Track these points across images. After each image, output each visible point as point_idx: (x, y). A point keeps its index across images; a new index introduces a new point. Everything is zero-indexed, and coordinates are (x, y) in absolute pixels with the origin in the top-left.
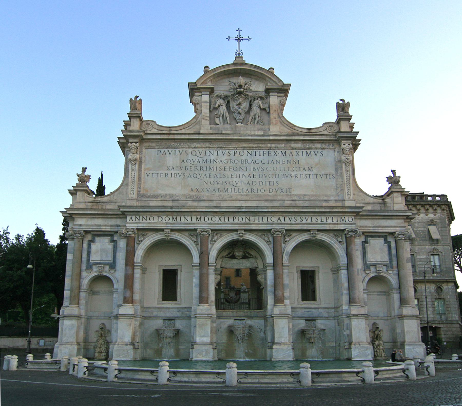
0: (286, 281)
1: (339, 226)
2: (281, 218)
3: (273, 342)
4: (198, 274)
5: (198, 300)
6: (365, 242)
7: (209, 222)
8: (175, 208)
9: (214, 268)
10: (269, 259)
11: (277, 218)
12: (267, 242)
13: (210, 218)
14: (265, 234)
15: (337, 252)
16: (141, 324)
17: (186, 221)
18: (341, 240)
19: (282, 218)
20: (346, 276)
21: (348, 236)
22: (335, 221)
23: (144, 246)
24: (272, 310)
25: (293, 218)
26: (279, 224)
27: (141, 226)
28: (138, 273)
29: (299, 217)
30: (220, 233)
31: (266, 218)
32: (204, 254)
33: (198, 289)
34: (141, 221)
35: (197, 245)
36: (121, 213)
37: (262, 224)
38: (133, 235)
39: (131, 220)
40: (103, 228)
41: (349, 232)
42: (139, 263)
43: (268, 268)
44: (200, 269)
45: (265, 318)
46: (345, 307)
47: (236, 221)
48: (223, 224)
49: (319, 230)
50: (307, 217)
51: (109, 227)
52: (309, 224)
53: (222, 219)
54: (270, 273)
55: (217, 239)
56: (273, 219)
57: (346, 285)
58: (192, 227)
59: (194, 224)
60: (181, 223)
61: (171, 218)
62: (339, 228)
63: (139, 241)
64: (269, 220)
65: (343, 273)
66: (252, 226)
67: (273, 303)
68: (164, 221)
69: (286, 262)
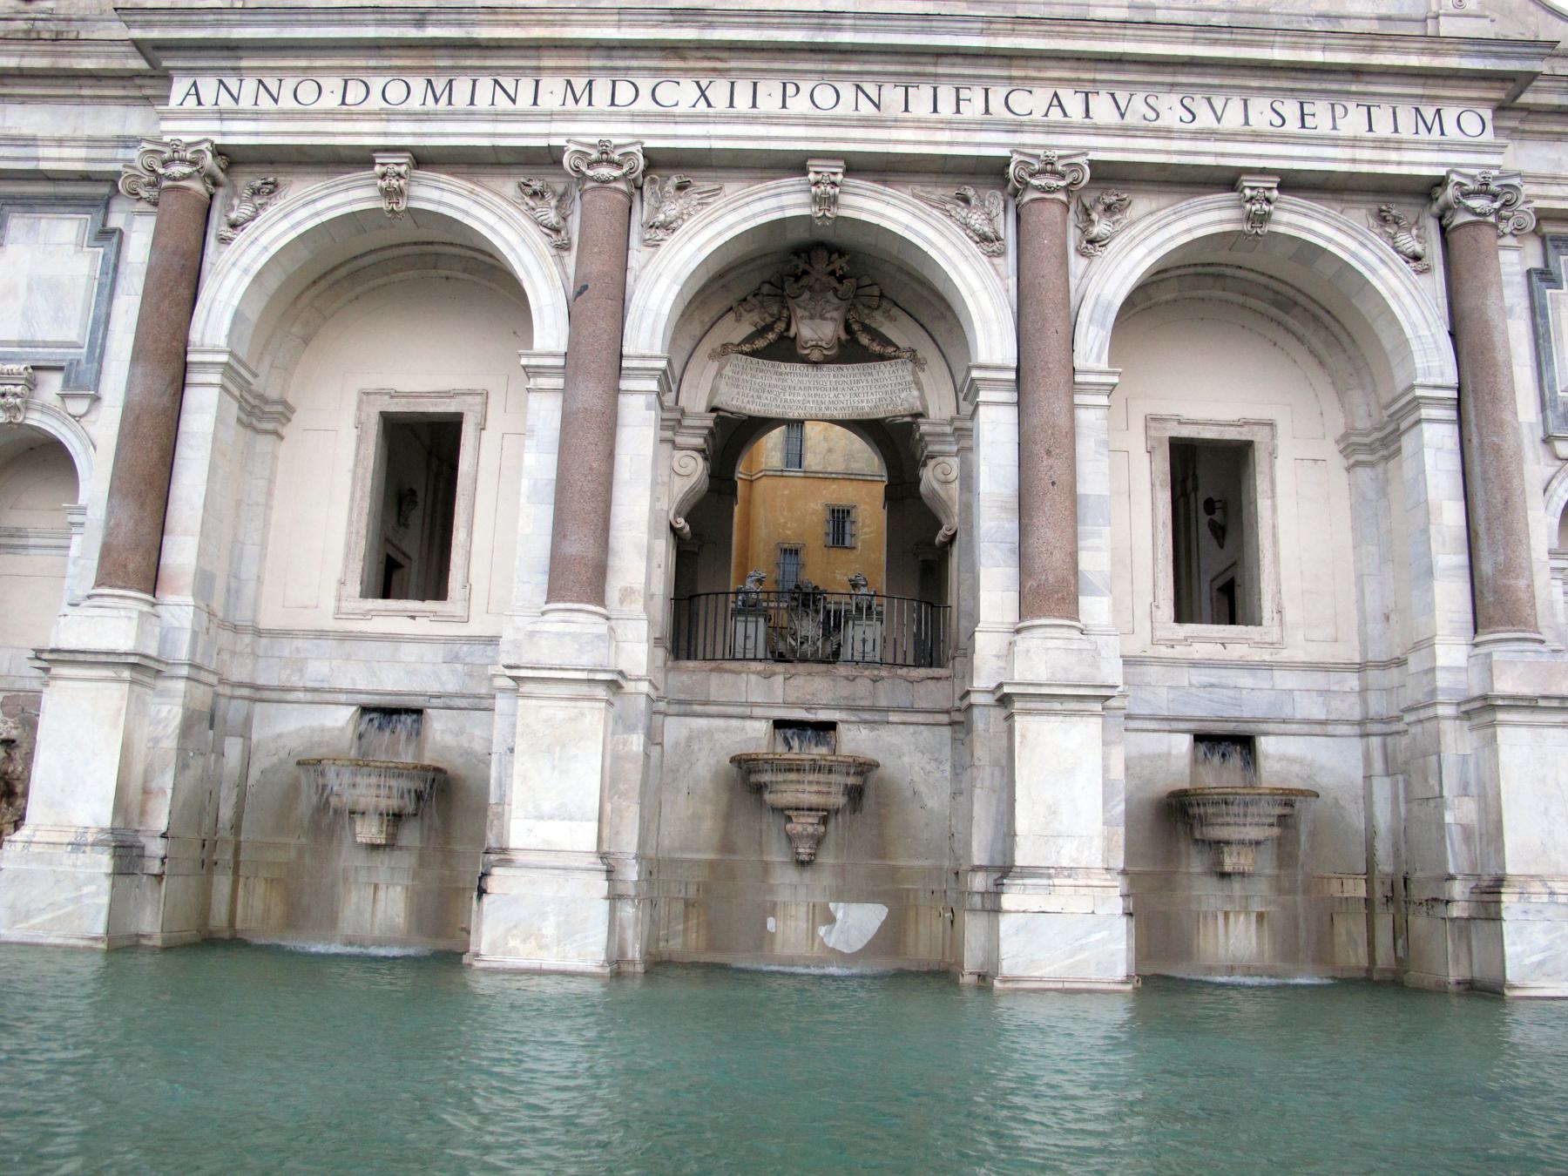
1: (1407, 156)
3: (1004, 871)
4: (556, 423)
5: (542, 580)
6: (1544, 276)
7: (635, 107)
8: (439, 24)
9: (653, 385)
11: (1042, 96)
12: (984, 239)
13: (645, 85)
14: (970, 192)
15: (1394, 320)
16: (204, 725)
17: (503, 103)
18: (1418, 248)
19: (1073, 102)
20: (1453, 463)
21: (1461, 218)
22: (1383, 129)
24: (1009, 653)
26: (1051, 128)
27: (241, 134)
28: (203, 408)
29: (1174, 99)
31: (977, 95)
32: (601, 299)
33: (546, 513)
34: (246, 103)
35: (563, 247)
36: (138, 64)
37: (948, 125)
39: (192, 101)
40: (52, 159)
41: (1466, 195)
43: (983, 396)
44: (566, 393)
46: (1451, 652)
49: (1292, 183)
50: (1218, 102)
51: (82, 153)
52: (1231, 137)
54: (996, 428)
56: (1021, 101)
57: (1450, 515)
59: (551, 116)
60: (470, 115)
61: (418, 84)
62: (1405, 170)
63: (234, 226)
65: (1436, 442)
67: (1011, 615)
68: (375, 102)
69: (1092, 364)
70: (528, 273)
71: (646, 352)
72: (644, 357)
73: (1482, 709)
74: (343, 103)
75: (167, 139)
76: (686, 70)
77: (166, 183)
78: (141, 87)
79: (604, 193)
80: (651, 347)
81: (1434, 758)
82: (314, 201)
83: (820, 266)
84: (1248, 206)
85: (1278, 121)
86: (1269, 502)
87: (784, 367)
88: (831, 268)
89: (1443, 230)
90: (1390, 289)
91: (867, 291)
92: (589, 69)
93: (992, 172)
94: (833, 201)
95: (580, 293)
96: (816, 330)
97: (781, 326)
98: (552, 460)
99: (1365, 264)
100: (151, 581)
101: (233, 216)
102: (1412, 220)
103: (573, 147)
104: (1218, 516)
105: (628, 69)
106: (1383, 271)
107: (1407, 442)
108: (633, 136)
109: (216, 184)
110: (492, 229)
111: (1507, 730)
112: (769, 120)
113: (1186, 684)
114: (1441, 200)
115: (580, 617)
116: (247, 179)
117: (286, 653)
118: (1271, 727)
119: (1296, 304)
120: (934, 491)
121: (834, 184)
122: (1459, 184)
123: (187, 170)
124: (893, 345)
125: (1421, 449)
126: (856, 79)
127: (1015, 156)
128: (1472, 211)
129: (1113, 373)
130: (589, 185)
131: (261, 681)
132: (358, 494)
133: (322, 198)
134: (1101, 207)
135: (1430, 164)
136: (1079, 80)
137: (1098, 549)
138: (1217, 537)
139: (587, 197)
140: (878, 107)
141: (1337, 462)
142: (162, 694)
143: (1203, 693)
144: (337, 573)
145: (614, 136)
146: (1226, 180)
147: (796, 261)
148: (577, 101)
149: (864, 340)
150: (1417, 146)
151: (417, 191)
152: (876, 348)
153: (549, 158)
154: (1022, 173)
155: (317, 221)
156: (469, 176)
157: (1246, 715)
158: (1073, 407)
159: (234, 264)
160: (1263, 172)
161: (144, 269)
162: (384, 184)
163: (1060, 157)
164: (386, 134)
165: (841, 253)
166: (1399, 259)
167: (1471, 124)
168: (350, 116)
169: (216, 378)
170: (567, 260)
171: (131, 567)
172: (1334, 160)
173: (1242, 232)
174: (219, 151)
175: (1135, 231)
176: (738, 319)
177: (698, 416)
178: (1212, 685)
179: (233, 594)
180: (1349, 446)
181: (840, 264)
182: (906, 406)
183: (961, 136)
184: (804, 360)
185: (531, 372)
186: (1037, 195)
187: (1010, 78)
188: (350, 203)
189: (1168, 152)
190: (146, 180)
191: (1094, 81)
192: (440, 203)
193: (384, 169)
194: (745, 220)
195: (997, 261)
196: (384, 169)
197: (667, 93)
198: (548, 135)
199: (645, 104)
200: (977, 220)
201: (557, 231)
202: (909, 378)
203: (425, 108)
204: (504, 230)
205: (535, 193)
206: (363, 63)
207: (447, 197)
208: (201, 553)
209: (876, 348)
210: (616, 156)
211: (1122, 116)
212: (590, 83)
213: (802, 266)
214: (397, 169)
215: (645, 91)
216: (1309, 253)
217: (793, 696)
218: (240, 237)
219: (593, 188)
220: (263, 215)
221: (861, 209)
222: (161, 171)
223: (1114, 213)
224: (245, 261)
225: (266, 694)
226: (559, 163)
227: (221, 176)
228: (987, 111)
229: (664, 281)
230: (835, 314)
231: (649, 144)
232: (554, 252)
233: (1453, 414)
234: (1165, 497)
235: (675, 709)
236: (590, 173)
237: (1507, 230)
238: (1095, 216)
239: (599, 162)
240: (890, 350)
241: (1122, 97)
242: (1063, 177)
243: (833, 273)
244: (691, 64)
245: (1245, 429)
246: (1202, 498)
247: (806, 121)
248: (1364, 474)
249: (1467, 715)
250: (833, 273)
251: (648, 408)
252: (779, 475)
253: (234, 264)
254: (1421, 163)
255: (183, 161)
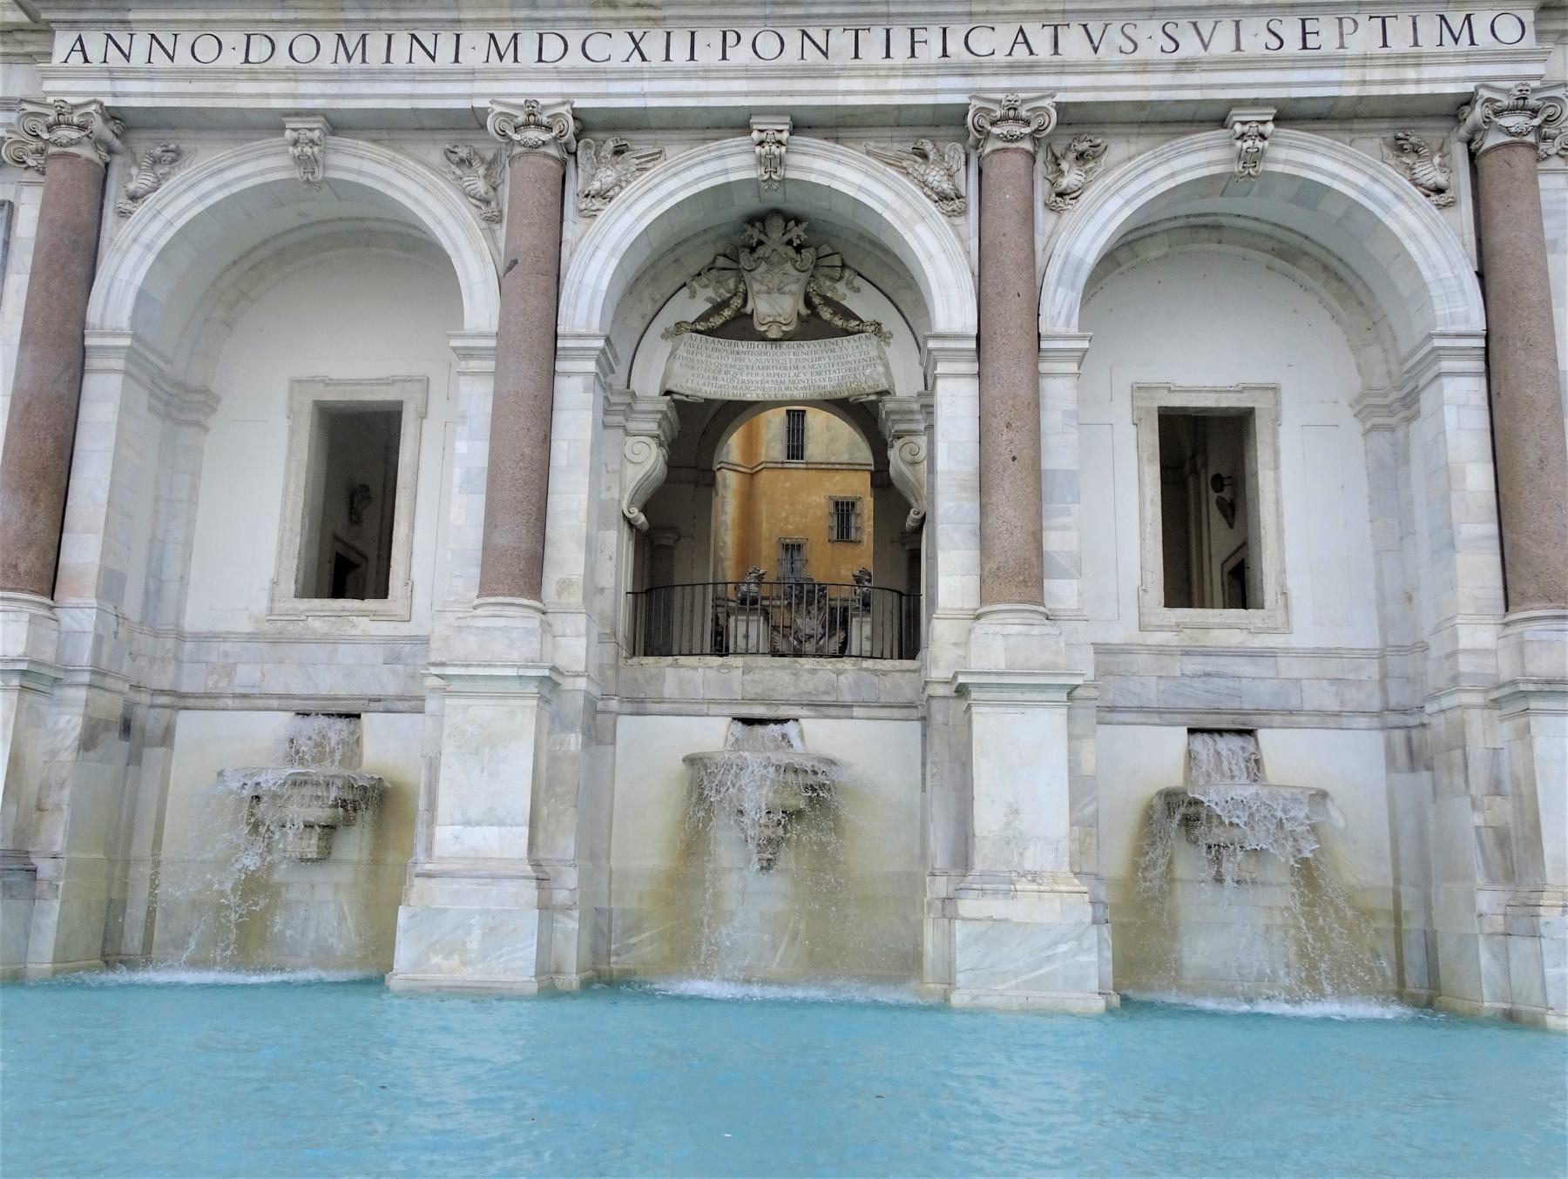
0: (1059, 453)
1: (1427, 72)
2: (1033, 30)
5: (475, 572)
9: (591, 366)
10: (952, 306)
11: (1006, 33)
12: (943, 197)
15: (1411, 264)
18: (1441, 180)
21: (1491, 140)
23: (156, 226)
25: (1115, 28)
26: (1013, 68)
27: (136, 94)
29: (1156, 26)
30: (641, 144)
31: (934, 37)
33: (479, 502)
34: (138, 59)
35: (493, 219)
37: (906, 72)
38: (86, 152)
39: (77, 58)
42: (117, 333)
43: (941, 368)
44: (497, 374)
45: (917, 709)
47: (741, 55)
48: (657, 75)
49: (1288, 115)
52: (1222, 64)
53: (653, 45)
54: (956, 402)
55: (618, 184)
56: (981, 42)
57: (1478, 479)
58: (452, 95)
61: (328, 40)
62: (1425, 89)
63: (134, 198)
64: (955, 45)
66: (842, 84)
67: (972, 602)
69: (1060, 329)
70: (457, 249)
71: (583, 331)
72: (580, 336)
73: (1515, 698)
74: (247, 61)
75: (50, 100)
76: (618, 20)
77: (52, 150)
78: (22, 43)
79: (531, 158)
80: (588, 324)
81: (1458, 752)
82: (221, 171)
83: (776, 233)
84: (1239, 143)
85: (1275, 43)
86: (1271, 474)
87: (743, 346)
88: (786, 238)
89: (1472, 156)
90: (1406, 227)
91: (826, 262)
92: (514, 20)
93: (950, 120)
94: (781, 161)
95: (509, 269)
96: (774, 304)
97: (737, 302)
98: (483, 447)
99: (1377, 201)
100: (49, 582)
101: (132, 186)
102: (1436, 147)
103: (498, 109)
104: (1227, 494)
105: (556, 20)
106: (1399, 208)
107: (1427, 400)
108: (563, 95)
109: (110, 152)
110: (416, 200)
111: (1544, 720)
112: (706, 74)
113: (1178, 674)
114: (1469, 122)
115: (510, 611)
116: (145, 145)
117: (213, 658)
118: (1277, 719)
119: (1306, 253)
120: (901, 475)
121: (780, 143)
122: (1488, 100)
123: (75, 135)
124: (856, 318)
125: (1441, 406)
126: (802, 24)
127: (974, 102)
128: (1507, 131)
129: (1082, 338)
130: (518, 150)
131: (185, 689)
132: (292, 488)
133: (230, 167)
134: (1072, 156)
135: (1455, 80)
136: (1047, 12)
137: (1066, 528)
138: (1225, 516)
139: (516, 165)
140: (825, 54)
141: (1355, 428)
142: (60, 703)
143: (1197, 683)
144: (269, 573)
145: (542, 95)
146: (1216, 117)
147: (750, 231)
148: (501, 58)
149: (826, 314)
150: (1440, 59)
151: (334, 159)
152: (838, 322)
153: (473, 120)
154: (983, 122)
155: (226, 193)
156: (390, 143)
157: (1247, 706)
158: (1037, 376)
159: (135, 240)
160: (1256, 103)
161: (32, 245)
162: (297, 151)
163: (1024, 101)
164: (294, 96)
165: (798, 221)
166: (1417, 193)
167: (1508, 29)
168: (254, 76)
169: (120, 364)
170: (498, 234)
171: (22, 567)
172: (1339, 84)
173: (1232, 175)
174: (113, 116)
175: (1109, 180)
176: (693, 295)
177: (651, 400)
178: (1207, 675)
179: (153, 595)
180: (1364, 407)
181: (797, 233)
182: (871, 383)
183: (914, 83)
184: (763, 338)
185: (466, 354)
186: (1000, 145)
187: (971, 14)
188: (262, 172)
189: (1146, 88)
190: (33, 147)
191: (1064, 12)
192: (359, 172)
193: (295, 135)
194: (687, 185)
195: (957, 221)
196: (295, 135)
197: (597, 47)
198: (471, 96)
199: (574, 59)
200: (936, 177)
201: (487, 203)
202: (874, 353)
203: (336, 67)
204: (430, 202)
205: (462, 161)
206: (266, 16)
207: (368, 166)
208: (105, 552)
209: (838, 322)
210: (544, 119)
211: (1096, 50)
212: (515, 36)
213: (757, 236)
214: (309, 134)
215: (574, 46)
216: (1309, 193)
217: (752, 691)
218: (141, 210)
219: (521, 155)
220: (165, 186)
221: (811, 170)
222: (46, 136)
223: (1087, 161)
224: (147, 237)
225: (190, 702)
226: (483, 127)
227: (117, 143)
228: (945, 55)
229: (601, 255)
230: (794, 288)
231: (579, 104)
232: (484, 225)
233: (1481, 366)
234: (1153, 473)
235: (628, 707)
236: (517, 137)
237: (1554, 151)
238: (1065, 166)
239: (527, 125)
240: (853, 323)
241: (1095, 28)
242: (1027, 123)
243: (790, 243)
244: (622, 13)
245: (1246, 394)
246: (1212, 472)
247: (748, 73)
248: (1381, 441)
249: (1496, 703)
250: (790, 243)
251: (586, 390)
252: (778, 467)
253: (135, 240)
254: (1446, 80)
255: (69, 125)
